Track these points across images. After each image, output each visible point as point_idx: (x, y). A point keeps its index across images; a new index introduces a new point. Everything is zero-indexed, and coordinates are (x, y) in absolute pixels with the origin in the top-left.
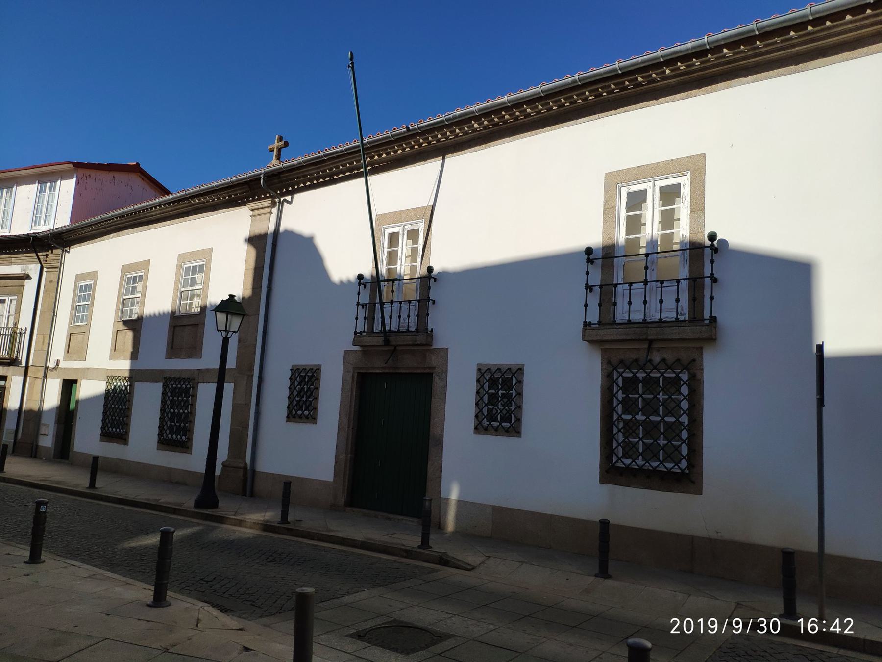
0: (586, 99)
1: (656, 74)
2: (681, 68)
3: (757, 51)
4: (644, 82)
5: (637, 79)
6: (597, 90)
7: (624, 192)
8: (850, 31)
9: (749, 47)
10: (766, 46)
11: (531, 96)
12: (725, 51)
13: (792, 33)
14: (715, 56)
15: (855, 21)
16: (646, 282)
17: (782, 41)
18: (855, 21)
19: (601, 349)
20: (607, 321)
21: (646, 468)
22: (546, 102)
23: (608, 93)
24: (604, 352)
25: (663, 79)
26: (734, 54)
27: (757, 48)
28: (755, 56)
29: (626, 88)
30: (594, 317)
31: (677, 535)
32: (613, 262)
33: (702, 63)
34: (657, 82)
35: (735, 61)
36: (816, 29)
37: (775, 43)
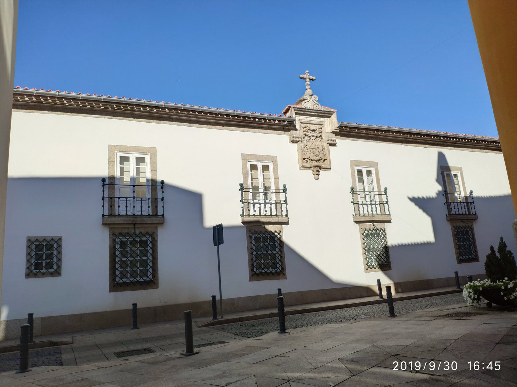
0: (100, 107)
1: (137, 108)
2: (148, 110)
3: (178, 114)
4: (130, 109)
5: (134, 108)
6: (107, 105)
7: (118, 155)
8: (208, 119)
9: (175, 112)
10: (181, 113)
11: (46, 94)
12: (167, 110)
13: (191, 113)
14: (163, 110)
15: (210, 116)
16: (134, 198)
17: (187, 114)
18: (210, 116)
19: (109, 228)
20: (111, 215)
21: (134, 281)
22: (77, 101)
23: (112, 108)
24: (111, 229)
25: (138, 111)
26: (170, 112)
27: (178, 113)
28: (177, 115)
29: (121, 109)
30: (106, 213)
31: (148, 308)
32: (115, 187)
33: (157, 111)
34: (136, 111)
35: (169, 115)
36: (199, 114)
37: (185, 114)
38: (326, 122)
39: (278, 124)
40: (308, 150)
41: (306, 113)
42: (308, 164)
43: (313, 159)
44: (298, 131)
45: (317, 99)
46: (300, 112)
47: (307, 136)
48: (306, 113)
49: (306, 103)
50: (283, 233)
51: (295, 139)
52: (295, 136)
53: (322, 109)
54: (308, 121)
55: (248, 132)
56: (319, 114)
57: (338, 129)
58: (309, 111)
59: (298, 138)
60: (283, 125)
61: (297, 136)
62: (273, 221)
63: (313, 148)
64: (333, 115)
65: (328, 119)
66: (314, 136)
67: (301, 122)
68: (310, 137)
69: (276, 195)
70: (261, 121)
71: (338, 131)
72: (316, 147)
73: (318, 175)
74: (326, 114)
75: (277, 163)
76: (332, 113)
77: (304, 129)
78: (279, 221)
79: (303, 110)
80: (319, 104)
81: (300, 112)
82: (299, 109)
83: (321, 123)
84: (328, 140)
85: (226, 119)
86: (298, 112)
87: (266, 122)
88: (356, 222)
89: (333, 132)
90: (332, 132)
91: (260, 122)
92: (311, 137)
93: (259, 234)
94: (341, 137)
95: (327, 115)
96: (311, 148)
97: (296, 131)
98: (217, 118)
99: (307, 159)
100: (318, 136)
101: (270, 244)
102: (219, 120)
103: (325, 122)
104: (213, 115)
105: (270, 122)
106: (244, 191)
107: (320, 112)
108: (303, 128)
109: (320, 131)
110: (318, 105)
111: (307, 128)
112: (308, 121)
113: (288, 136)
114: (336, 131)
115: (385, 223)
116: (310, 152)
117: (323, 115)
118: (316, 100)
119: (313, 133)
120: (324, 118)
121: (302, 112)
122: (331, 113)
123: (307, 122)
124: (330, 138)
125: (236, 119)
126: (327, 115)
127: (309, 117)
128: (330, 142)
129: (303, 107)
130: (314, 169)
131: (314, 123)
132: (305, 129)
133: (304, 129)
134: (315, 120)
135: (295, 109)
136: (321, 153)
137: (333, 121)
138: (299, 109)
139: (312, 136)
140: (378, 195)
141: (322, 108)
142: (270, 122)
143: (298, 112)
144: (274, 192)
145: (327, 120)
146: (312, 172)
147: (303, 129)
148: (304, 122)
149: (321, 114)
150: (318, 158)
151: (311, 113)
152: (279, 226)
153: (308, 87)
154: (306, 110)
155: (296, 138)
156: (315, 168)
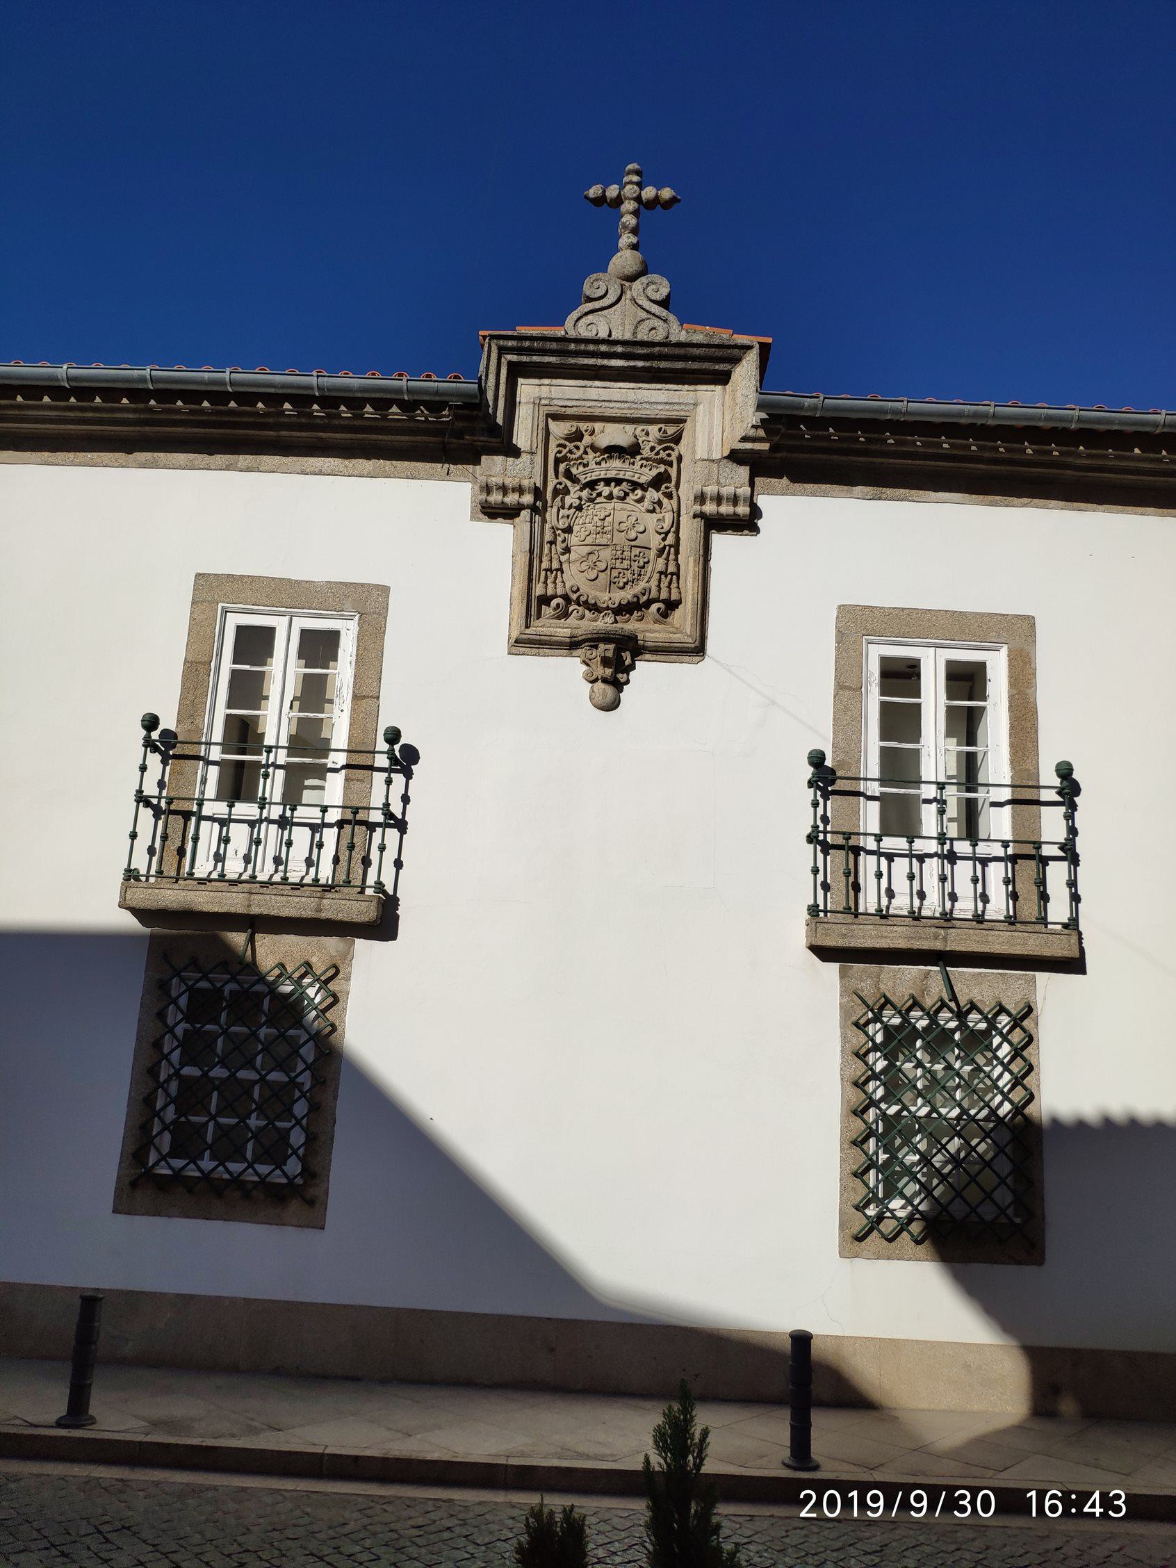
38: (701, 408)
39: (407, 424)
40: (573, 556)
41: (572, 361)
42: (562, 630)
43: (592, 601)
44: (525, 458)
45: (664, 291)
46: (536, 359)
47: (574, 480)
48: (572, 361)
49: (590, 318)
50: (348, 979)
51: (496, 498)
52: (494, 480)
53: (683, 337)
54: (588, 404)
55: (249, 470)
56: (655, 364)
57: (761, 433)
58: (591, 347)
59: (514, 490)
60: (431, 426)
61: (509, 482)
62: (285, 912)
63: (598, 542)
64: (744, 362)
65: (719, 388)
66: (618, 482)
67: (552, 410)
68: (592, 485)
69: (347, 779)
70: (310, 415)
71: (765, 446)
72: (620, 539)
73: (618, 686)
74: (694, 359)
75: (385, 618)
76: (736, 352)
77: (564, 446)
78: (324, 915)
79: (554, 346)
80: (672, 318)
81: (536, 359)
82: (527, 344)
83: (673, 413)
84: (701, 498)
85: (131, 416)
86: (524, 359)
87: (339, 416)
88: (824, 953)
89: (735, 457)
90: (726, 453)
91: (303, 420)
92: (601, 487)
93: (205, 977)
94: (794, 480)
95: (706, 365)
96: (589, 540)
97: (511, 460)
98: (90, 415)
99: (559, 600)
100: (643, 480)
101: (233, 1029)
102: (100, 422)
103: (695, 405)
104: (68, 400)
105: (356, 417)
106: (175, 757)
107: (657, 349)
108: (563, 442)
109: (663, 454)
110: (665, 321)
111: (587, 439)
112: (588, 404)
113: (470, 485)
114: (749, 446)
115: (1038, 974)
116: (584, 566)
117: (679, 365)
118: (657, 297)
119: (616, 463)
120: (690, 384)
121: (553, 359)
122: (733, 355)
123: (589, 412)
124: (711, 490)
125: (178, 411)
126: (706, 365)
127: (597, 383)
128: (710, 508)
129: (572, 334)
130: (594, 652)
131: (629, 413)
132: (570, 446)
133: (564, 446)
134: (631, 396)
135: (501, 342)
136: (649, 567)
137: (738, 394)
138: (527, 344)
139: (608, 482)
140: (1008, 808)
141: (679, 333)
142: (361, 417)
143: (524, 359)
144: (343, 767)
145: (709, 395)
146: (585, 668)
147: (559, 445)
148: (569, 411)
149: (663, 364)
150: (626, 595)
151: (605, 362)
152: (332, 944)
153: (626, 239)
154: (572, 347)
155: (505, 495)
156: (596, 647)
